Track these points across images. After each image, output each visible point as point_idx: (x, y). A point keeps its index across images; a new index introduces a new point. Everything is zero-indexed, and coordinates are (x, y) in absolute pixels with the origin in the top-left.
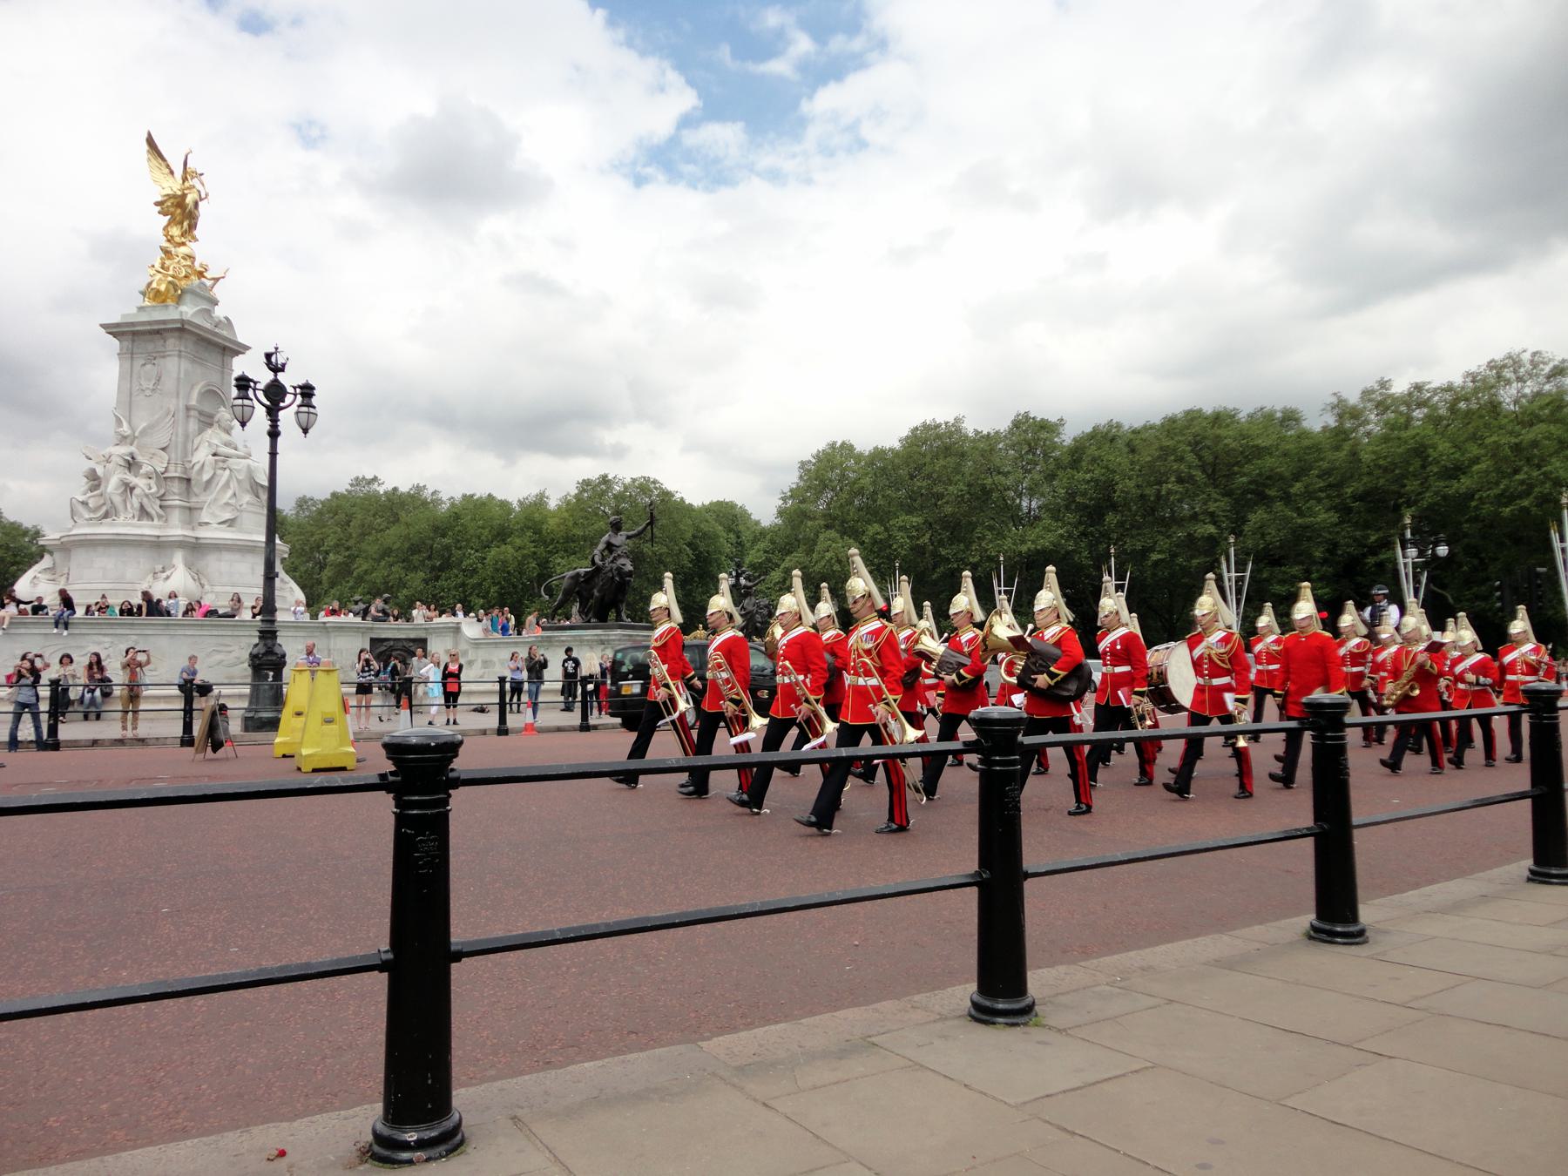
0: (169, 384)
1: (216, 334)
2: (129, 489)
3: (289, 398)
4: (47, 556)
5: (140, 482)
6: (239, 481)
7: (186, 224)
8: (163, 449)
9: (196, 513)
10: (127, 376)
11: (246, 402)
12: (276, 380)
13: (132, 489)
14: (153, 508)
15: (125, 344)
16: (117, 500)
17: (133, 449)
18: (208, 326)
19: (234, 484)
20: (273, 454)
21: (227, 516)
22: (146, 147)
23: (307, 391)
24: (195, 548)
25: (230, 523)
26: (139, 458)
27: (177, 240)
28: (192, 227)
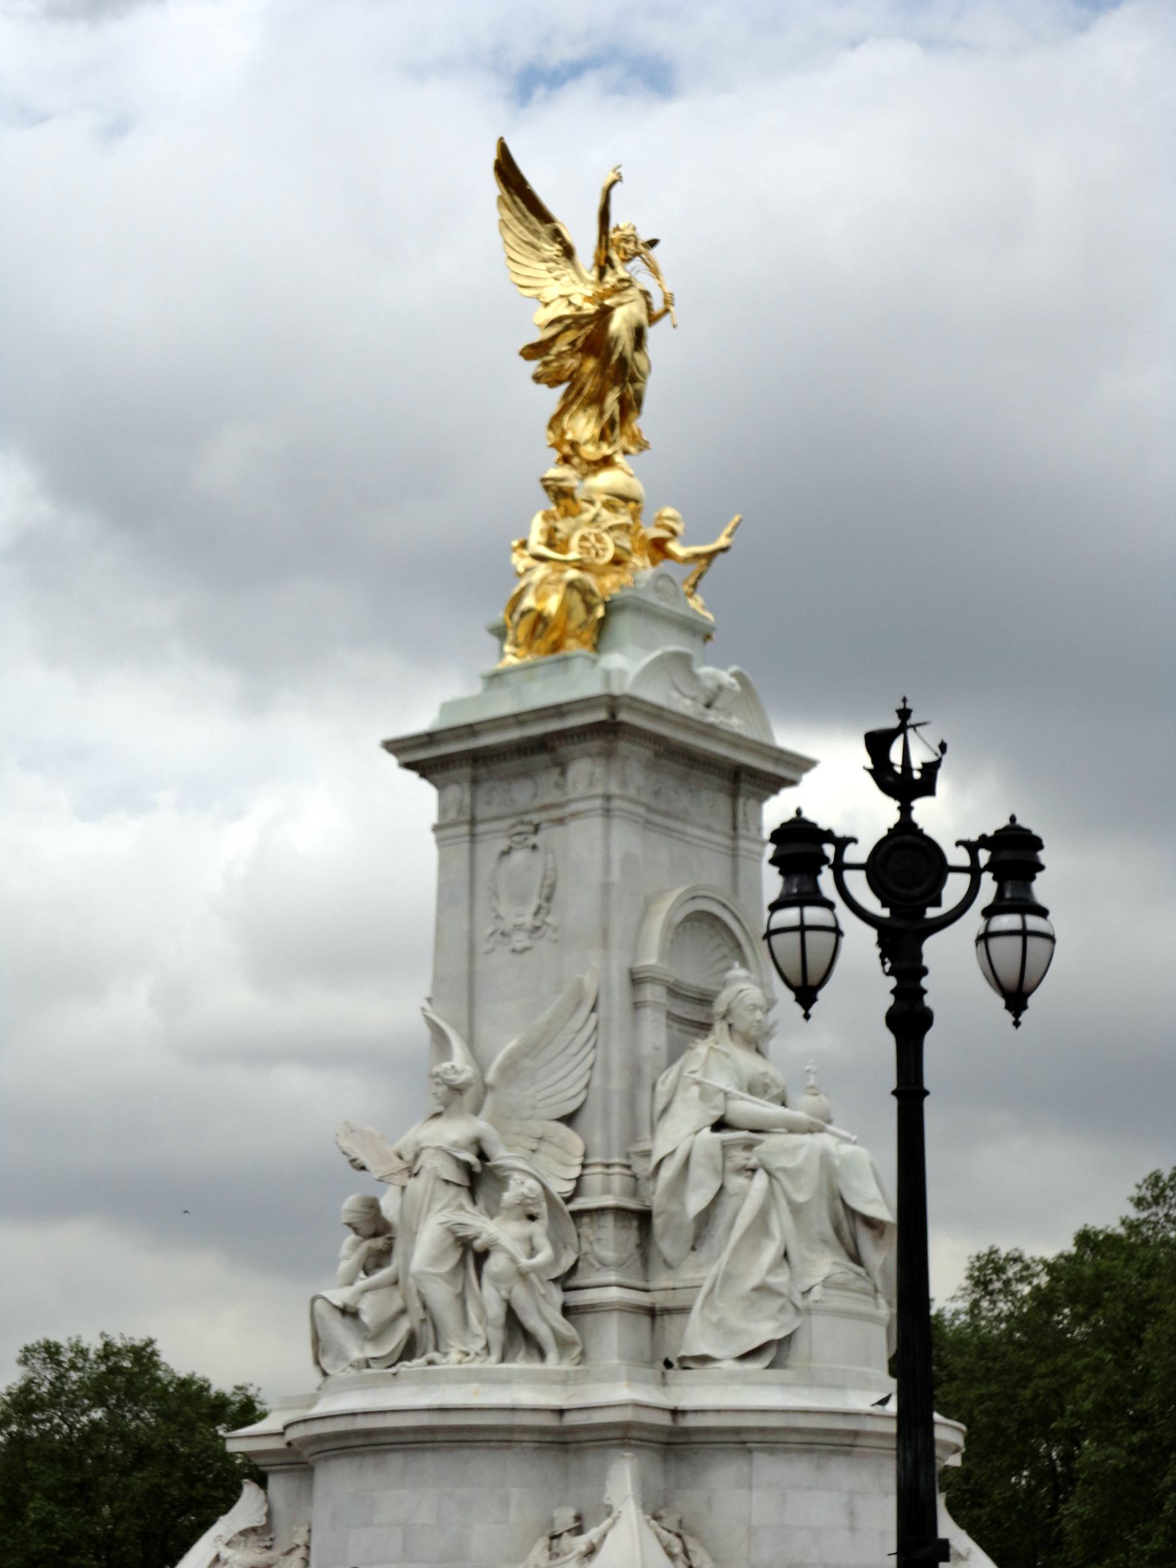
0: (578, 905)
1: (710, 731)
2: (472, 1255)
3: (954, 888)
4: (250, 1491)
5: (501, 1232)
6: (796, 1210)
8: (569, 1120)
9: (670, 1324)
10: (462, 889)
11: (814, 914)
12: (906, 827)
13: (481, 1257)
14: (543, 1317)
15: (454, 791)
16: (441, 1294)
17: (480, 1125)
18: (685, 706)
19: (781, 1223)
20: (910, 1095)
21: (765, 1330)
22: (492, 188)
23: (1013, 855)
24: (676, 1444)
25: (773, 1353)
26: (501, 1155)
27: (590, 452)
28: (630, 405)
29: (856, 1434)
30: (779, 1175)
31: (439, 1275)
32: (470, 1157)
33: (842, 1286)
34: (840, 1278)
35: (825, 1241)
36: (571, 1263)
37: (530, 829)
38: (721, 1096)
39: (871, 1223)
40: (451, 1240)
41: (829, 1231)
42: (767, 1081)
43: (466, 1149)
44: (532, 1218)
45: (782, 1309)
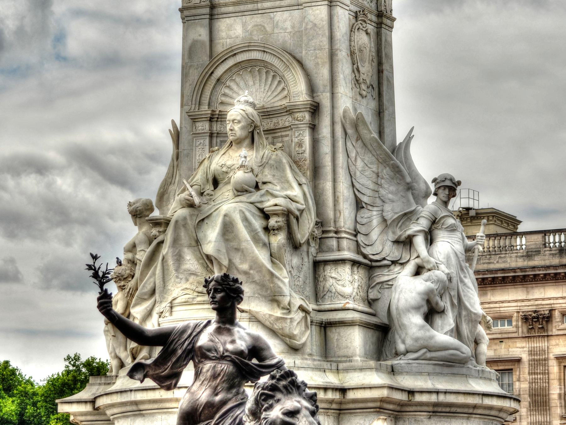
29: (136, 403)
33: (186, 303)
42: (224, 169)
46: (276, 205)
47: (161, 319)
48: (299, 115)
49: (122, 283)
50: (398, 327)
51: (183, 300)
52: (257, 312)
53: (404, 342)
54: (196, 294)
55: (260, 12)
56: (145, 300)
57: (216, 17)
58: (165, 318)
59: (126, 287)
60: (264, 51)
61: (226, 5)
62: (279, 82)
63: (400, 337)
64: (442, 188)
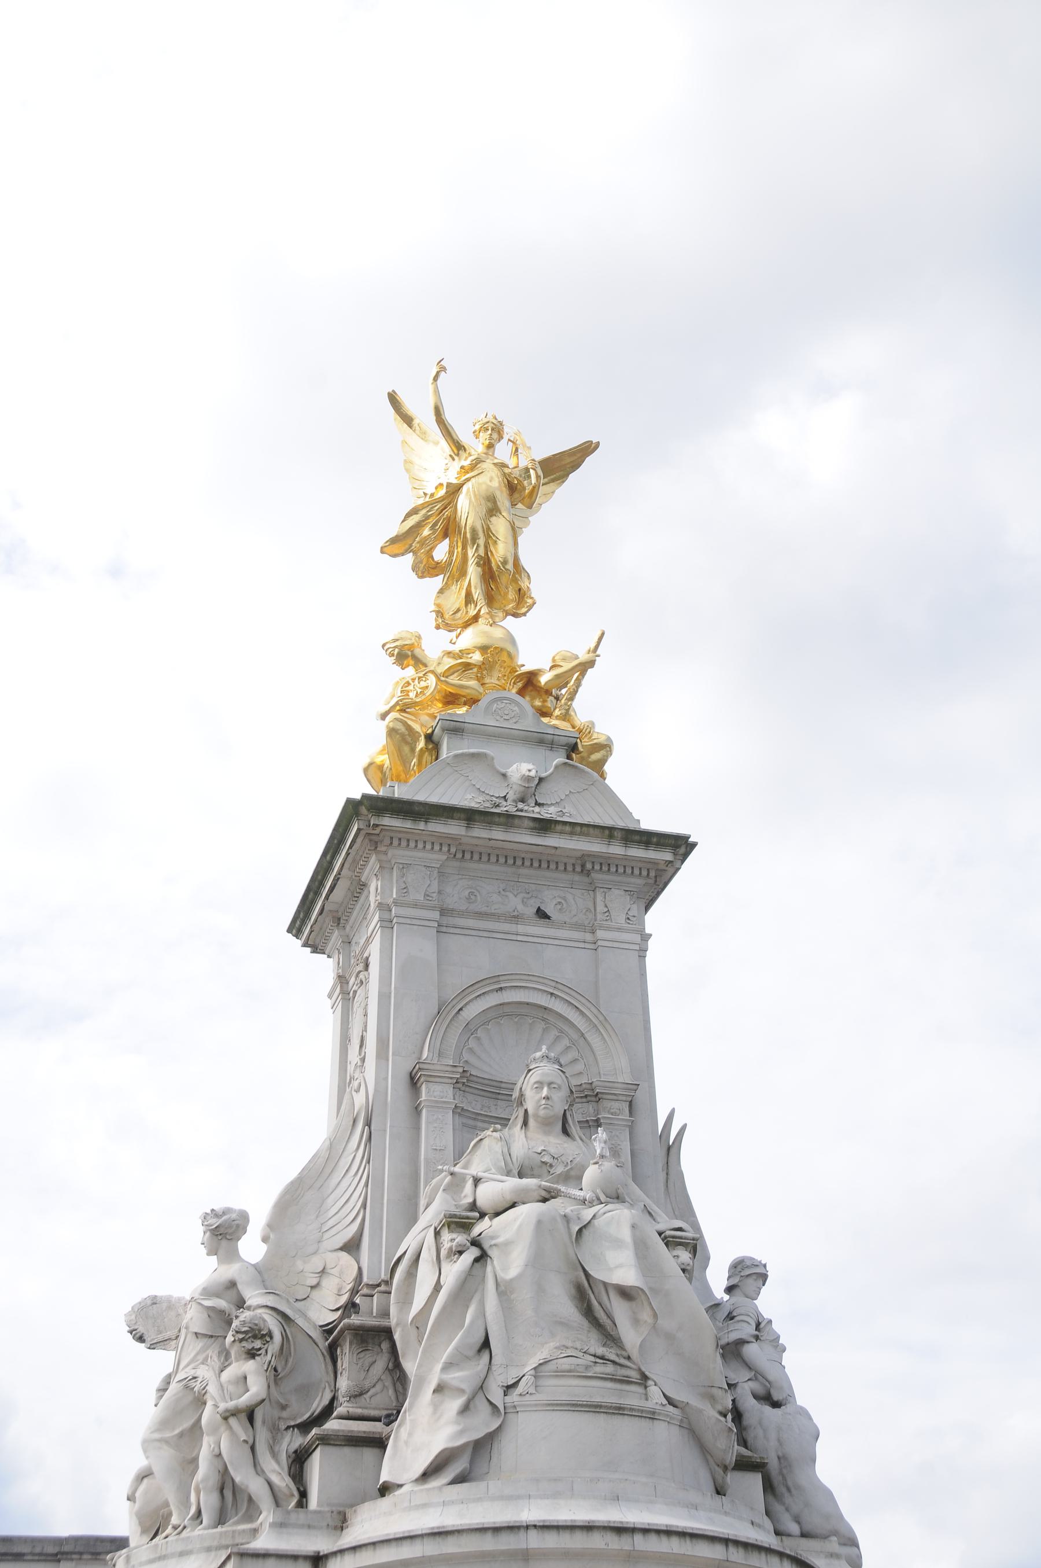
6: (504, 1290)
7: (473, 572)
8: (352, 1247)
30: (493, 1253)
31: (166, 1441)
32: (221, 1303)
34: (565, 1364)
35: (563, 1324)
36: (326, 1401)
37: (361, 967)
38: (470, 1183)
39: (626, 1293)
40: (190, 1398)
41: (569, 1310)
42: (546, 1159)
43: (218, 1295)
44: (252, 1354)
45: (465, 1409)
46: (680, 1229)
47: (508, 1399)
48: (616, 1105)
49: (258, 1344)
50: (783, 1490)
51: (566, 1367)
52: (701, 1411)
53: (797, 1520)
54: (593, 1359)
55: (519, 938)
56: (468, 1358)
57: (444, 929)
58: (528, 1397)
59: (263, 1351)
60: (552, 994)
61: (462, 914)
62: (568, 1048)
63: (787, 1510)
64: (754, 1277)
